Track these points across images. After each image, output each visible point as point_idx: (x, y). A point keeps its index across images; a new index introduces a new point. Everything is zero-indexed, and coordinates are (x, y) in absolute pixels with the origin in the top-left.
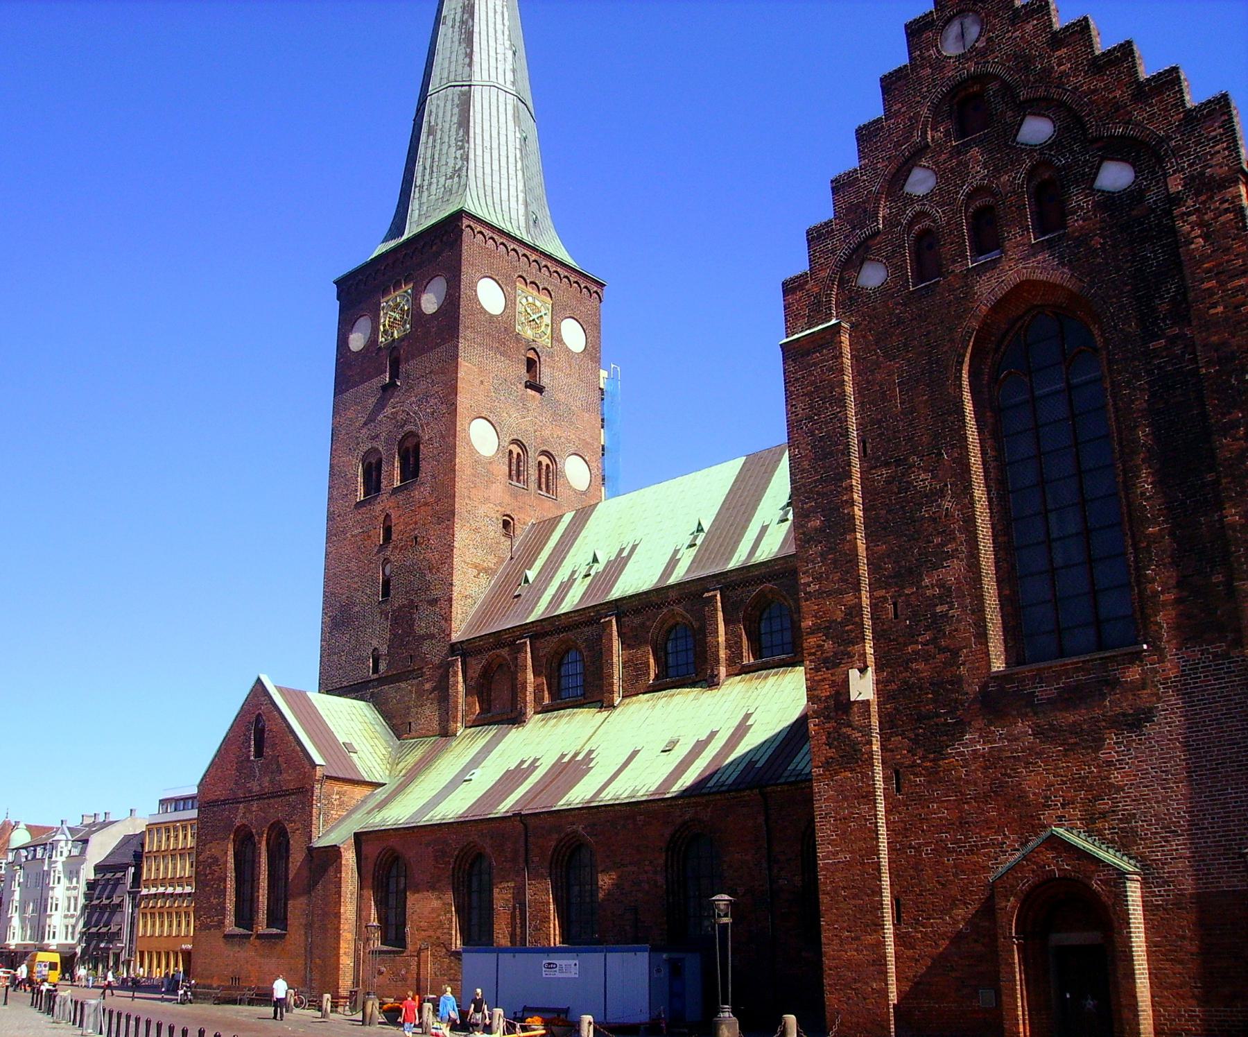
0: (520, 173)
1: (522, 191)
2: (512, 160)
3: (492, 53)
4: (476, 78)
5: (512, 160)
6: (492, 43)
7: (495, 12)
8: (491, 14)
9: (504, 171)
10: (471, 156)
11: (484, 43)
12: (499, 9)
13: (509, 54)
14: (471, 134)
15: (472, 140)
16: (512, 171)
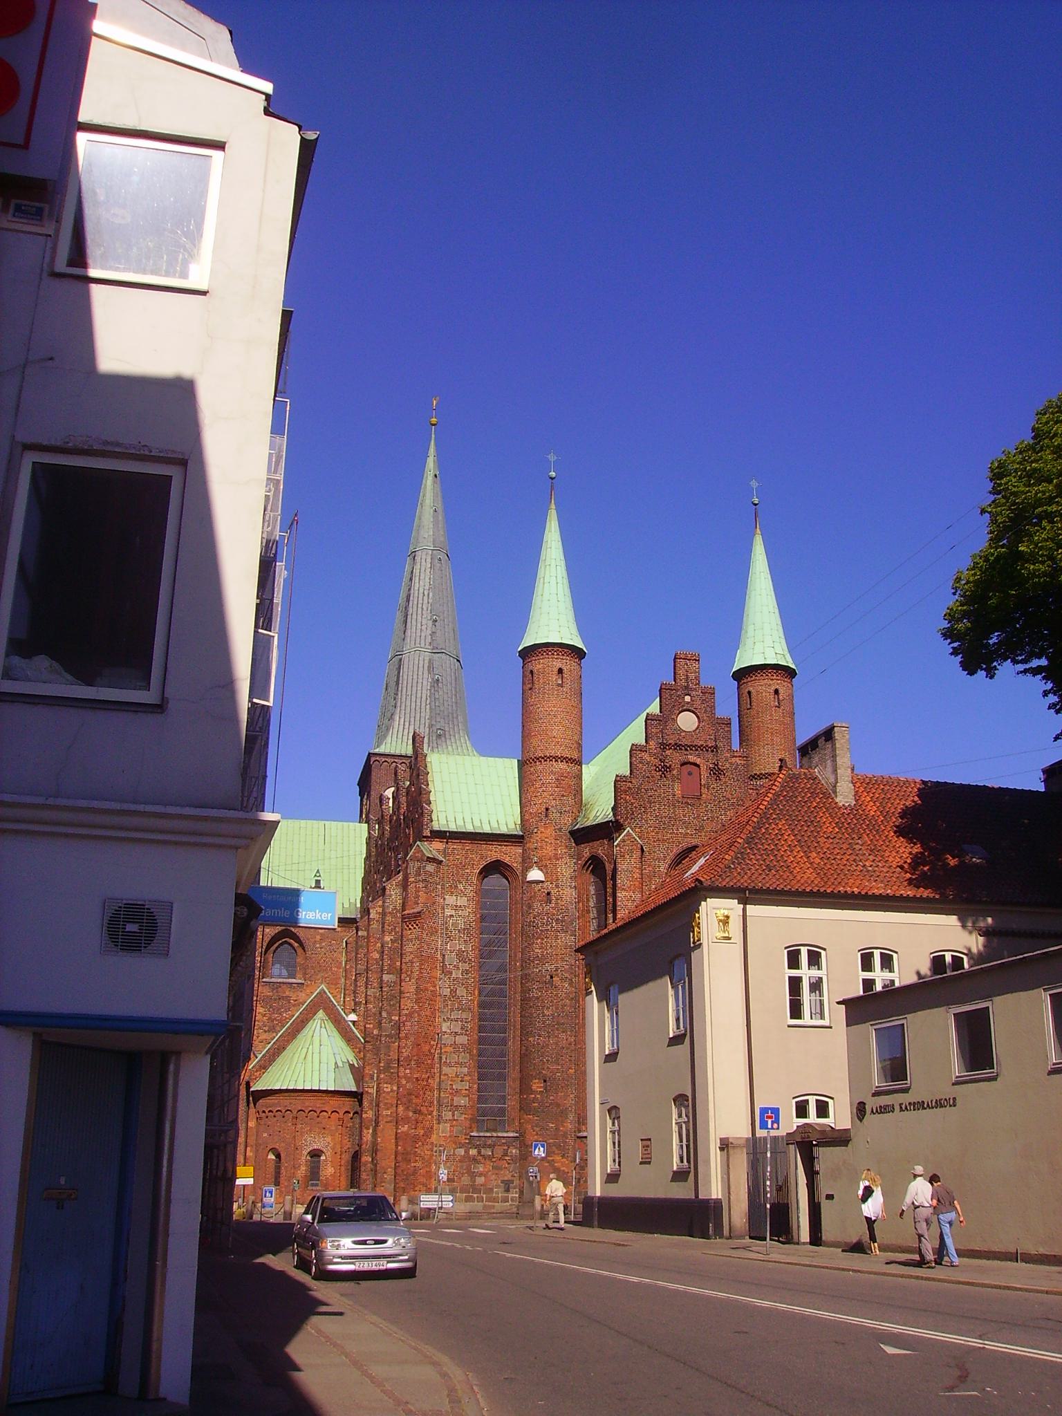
0: (428, 706)
1: (428, 719)
2: (424, 699)
3: (419, 625)
4: (406, 648)
5: (424, 699)
6: (419, 620)
7: (424, 595)
8: (421, 596)
9: (418, 708)
10: (399, 704)
11: (414, 623)
12: (426, 593)
13: (430, 623)
14: (400, 689)
15: (400, 695)
16: (423, 705)
